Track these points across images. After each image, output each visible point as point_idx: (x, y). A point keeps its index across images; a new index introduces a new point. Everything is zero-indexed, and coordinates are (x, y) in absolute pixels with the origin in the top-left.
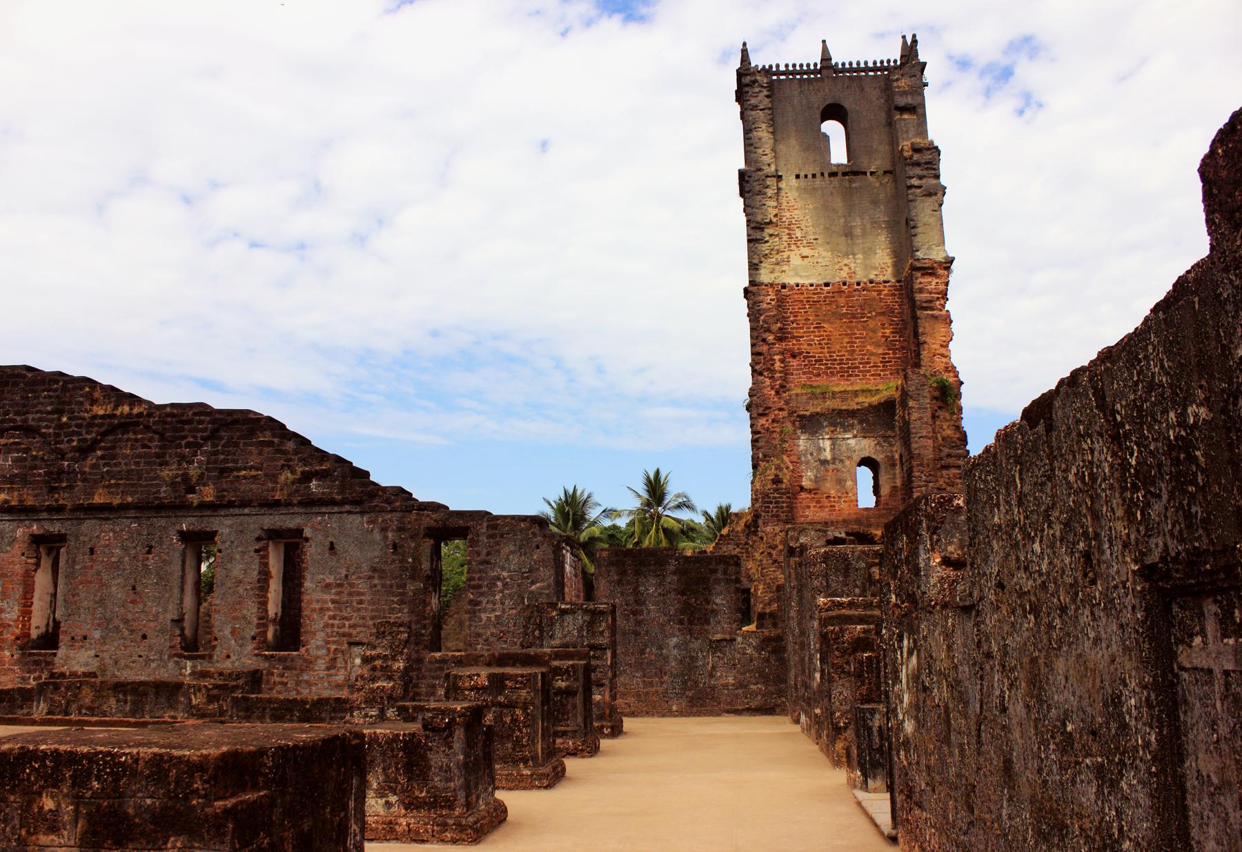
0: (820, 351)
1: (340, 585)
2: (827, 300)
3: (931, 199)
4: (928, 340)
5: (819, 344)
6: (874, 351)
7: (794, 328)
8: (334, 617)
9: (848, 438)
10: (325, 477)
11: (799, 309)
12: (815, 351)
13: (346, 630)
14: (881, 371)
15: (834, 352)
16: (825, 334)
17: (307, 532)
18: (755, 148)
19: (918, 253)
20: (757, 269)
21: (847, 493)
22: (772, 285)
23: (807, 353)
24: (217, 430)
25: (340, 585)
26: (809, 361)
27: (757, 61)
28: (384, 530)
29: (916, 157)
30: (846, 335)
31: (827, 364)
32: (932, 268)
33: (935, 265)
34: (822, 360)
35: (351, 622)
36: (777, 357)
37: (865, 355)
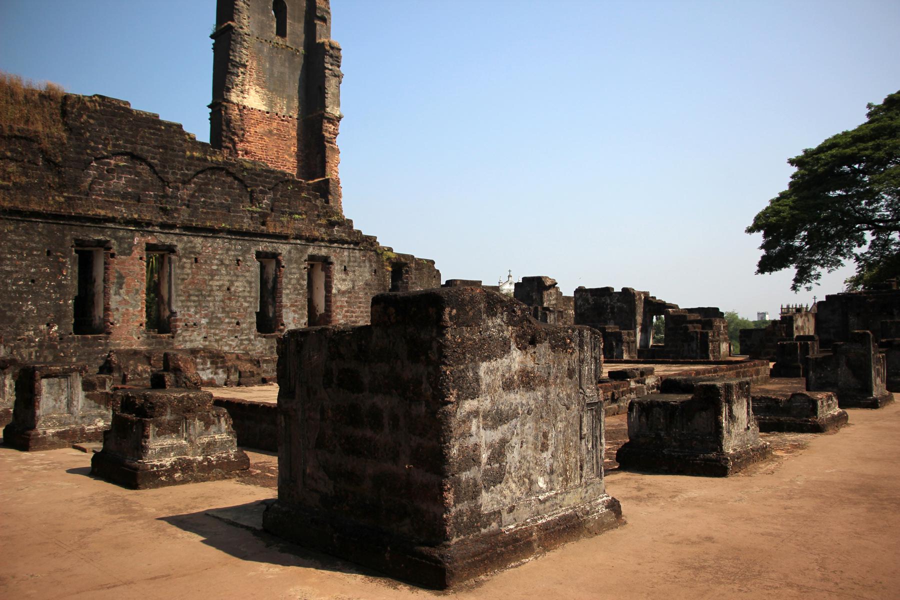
1: (350, 292)
4: (330, 161)
7: (248, 136)
8: (347, 312)
10: (341, 226)
13: (353, 319)
15: (268, 156)
17: (333, 259)
19: (328, 109)
20: (230, 92)
22: (238, 105)
24: (277, 185)
25: (350, 292)
26: (255, 158)
28: (370, 261)
29: (331, 52)
32: (333, 120)
34: (262, 159)
35: (356, 314)
37: (284, 160)
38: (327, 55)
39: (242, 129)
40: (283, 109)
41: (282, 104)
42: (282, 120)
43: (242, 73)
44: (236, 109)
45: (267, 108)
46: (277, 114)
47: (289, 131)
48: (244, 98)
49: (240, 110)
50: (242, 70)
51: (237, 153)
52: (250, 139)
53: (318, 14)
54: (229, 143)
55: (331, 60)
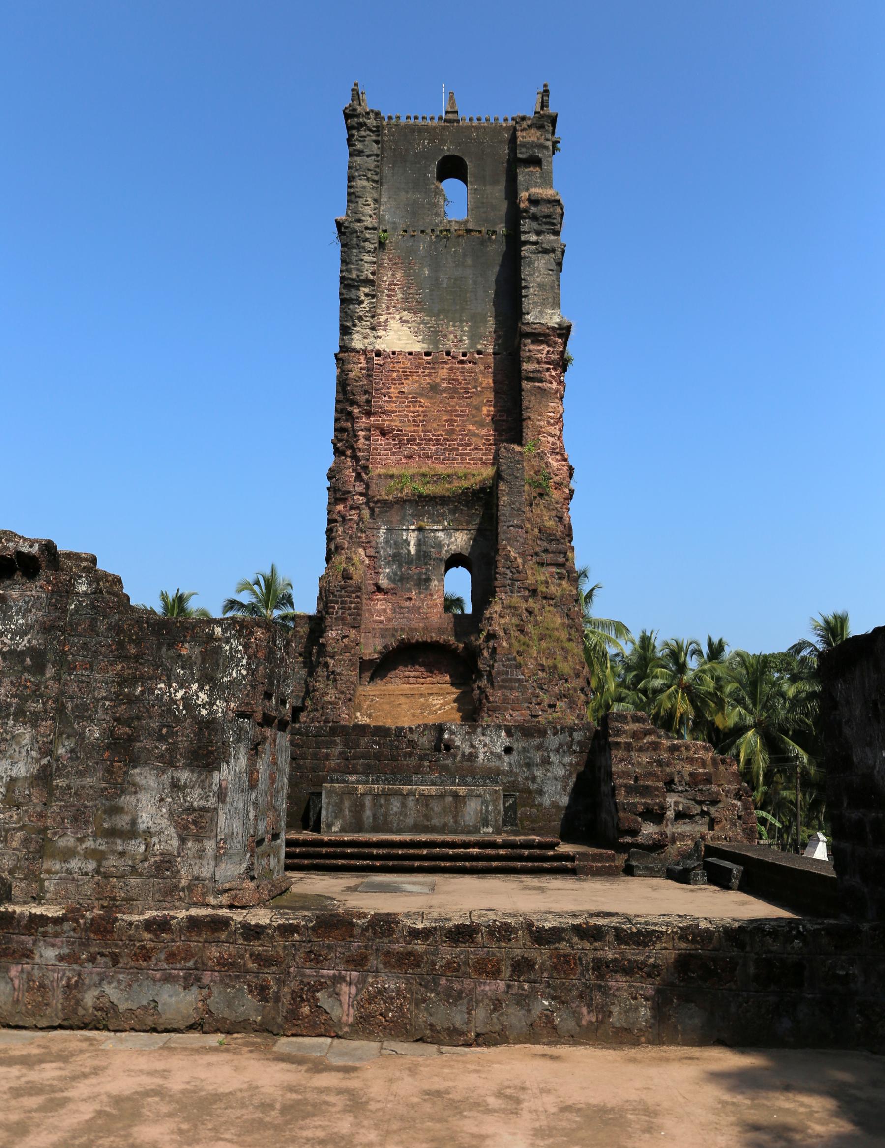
0: (413, 428)
3: (546, 257)
5: (414, 421)
6: (477, 431)
9: (436, 530)
14: (484, 454)
15: (430, 431)
16: (421, 409)
18: (356, 197)
19: (526, 317)
20: (350, 334)
21: (432, 595)
22: (364, 352)
23: (398, 430)
26: (400, 440)
27: (369, 103)
29: (533, 209)
30: (446, 411)
31: (421, 444)
32: (546, 335)
36: (361, 433)
37: (466, 435)
38: (525, 218)
39: (366, 392)
40: (461, 341)
41: (459, 333)
42: (462, 362)
43: (367, 295)
44: (362, 360)
45: (425, 346)
46: (448, 354)
47: (476, 380)
48: (376, 337)
49: (369, 360)
50: (367, 290)
51: (356, 436)
52: (389, 407)
53: (520, 156)
54: (347, 420)
55: (535, 225)
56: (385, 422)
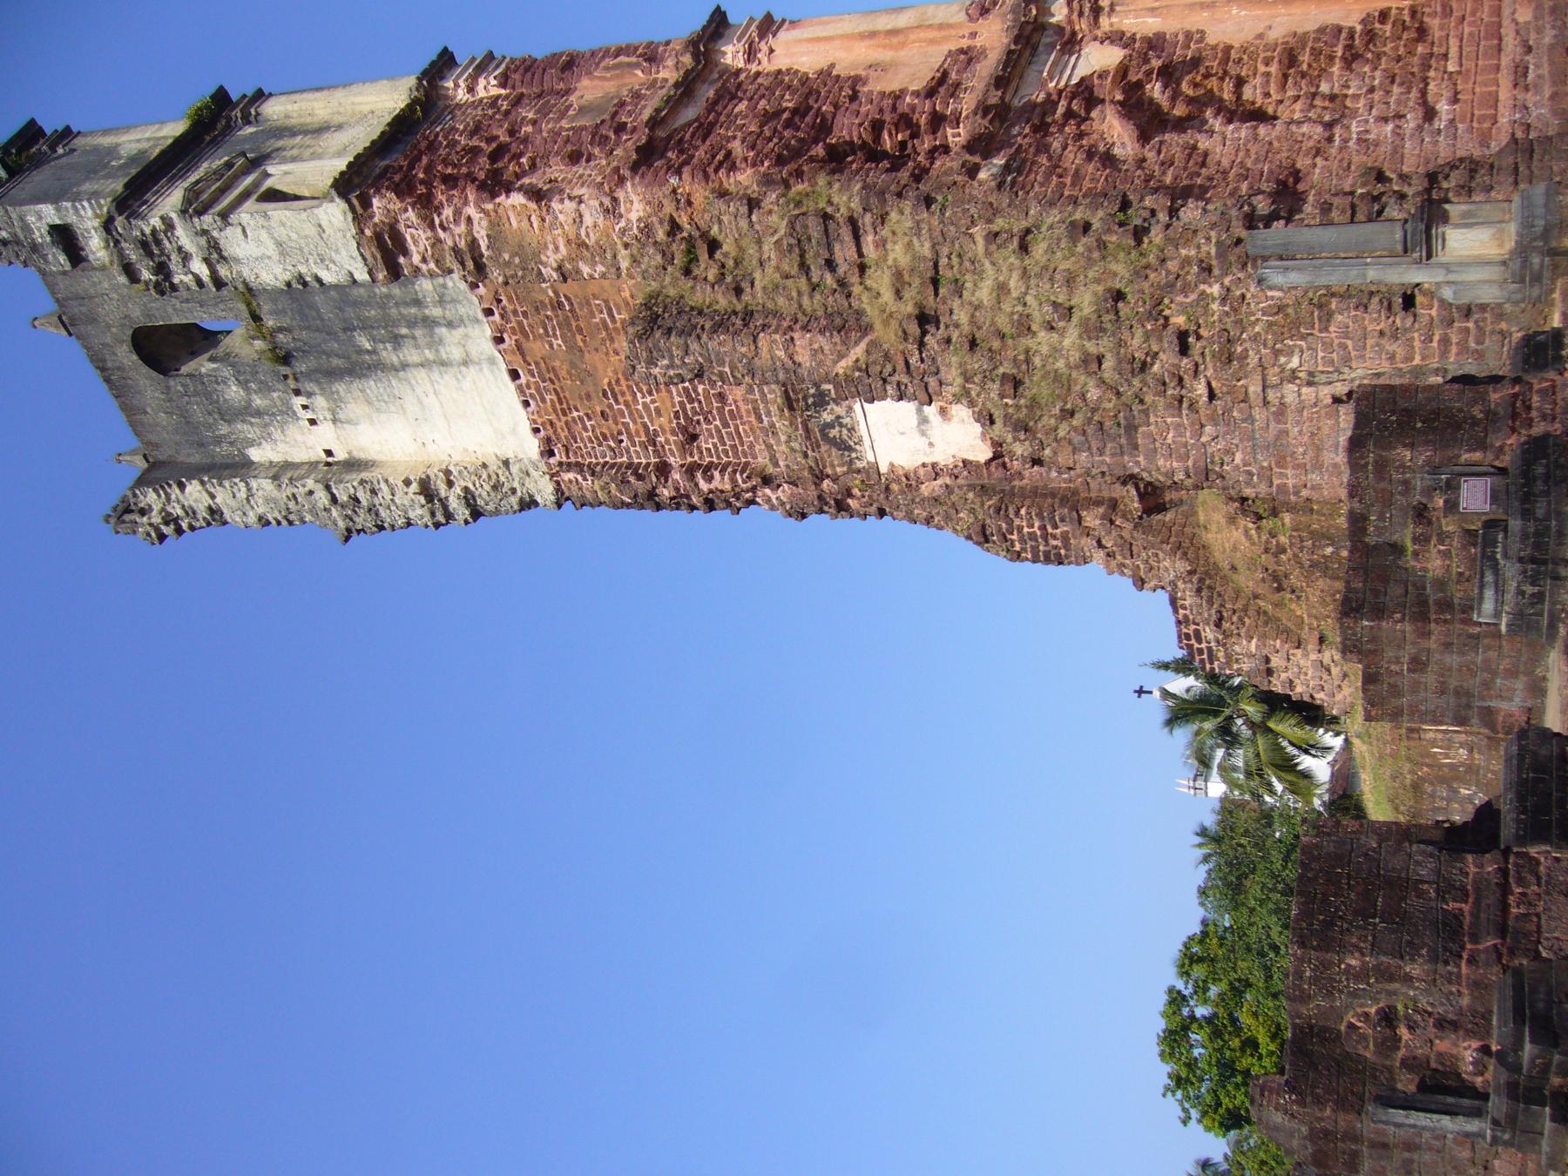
2: (547, 376)
5: (650, 393)
11: (586, 430)
12: (669, 404)
16: (623, 382)
23: (677, 417)
32: (378, 237)
33: (368, 232)
56: (670, 442)
